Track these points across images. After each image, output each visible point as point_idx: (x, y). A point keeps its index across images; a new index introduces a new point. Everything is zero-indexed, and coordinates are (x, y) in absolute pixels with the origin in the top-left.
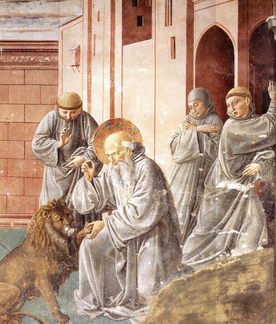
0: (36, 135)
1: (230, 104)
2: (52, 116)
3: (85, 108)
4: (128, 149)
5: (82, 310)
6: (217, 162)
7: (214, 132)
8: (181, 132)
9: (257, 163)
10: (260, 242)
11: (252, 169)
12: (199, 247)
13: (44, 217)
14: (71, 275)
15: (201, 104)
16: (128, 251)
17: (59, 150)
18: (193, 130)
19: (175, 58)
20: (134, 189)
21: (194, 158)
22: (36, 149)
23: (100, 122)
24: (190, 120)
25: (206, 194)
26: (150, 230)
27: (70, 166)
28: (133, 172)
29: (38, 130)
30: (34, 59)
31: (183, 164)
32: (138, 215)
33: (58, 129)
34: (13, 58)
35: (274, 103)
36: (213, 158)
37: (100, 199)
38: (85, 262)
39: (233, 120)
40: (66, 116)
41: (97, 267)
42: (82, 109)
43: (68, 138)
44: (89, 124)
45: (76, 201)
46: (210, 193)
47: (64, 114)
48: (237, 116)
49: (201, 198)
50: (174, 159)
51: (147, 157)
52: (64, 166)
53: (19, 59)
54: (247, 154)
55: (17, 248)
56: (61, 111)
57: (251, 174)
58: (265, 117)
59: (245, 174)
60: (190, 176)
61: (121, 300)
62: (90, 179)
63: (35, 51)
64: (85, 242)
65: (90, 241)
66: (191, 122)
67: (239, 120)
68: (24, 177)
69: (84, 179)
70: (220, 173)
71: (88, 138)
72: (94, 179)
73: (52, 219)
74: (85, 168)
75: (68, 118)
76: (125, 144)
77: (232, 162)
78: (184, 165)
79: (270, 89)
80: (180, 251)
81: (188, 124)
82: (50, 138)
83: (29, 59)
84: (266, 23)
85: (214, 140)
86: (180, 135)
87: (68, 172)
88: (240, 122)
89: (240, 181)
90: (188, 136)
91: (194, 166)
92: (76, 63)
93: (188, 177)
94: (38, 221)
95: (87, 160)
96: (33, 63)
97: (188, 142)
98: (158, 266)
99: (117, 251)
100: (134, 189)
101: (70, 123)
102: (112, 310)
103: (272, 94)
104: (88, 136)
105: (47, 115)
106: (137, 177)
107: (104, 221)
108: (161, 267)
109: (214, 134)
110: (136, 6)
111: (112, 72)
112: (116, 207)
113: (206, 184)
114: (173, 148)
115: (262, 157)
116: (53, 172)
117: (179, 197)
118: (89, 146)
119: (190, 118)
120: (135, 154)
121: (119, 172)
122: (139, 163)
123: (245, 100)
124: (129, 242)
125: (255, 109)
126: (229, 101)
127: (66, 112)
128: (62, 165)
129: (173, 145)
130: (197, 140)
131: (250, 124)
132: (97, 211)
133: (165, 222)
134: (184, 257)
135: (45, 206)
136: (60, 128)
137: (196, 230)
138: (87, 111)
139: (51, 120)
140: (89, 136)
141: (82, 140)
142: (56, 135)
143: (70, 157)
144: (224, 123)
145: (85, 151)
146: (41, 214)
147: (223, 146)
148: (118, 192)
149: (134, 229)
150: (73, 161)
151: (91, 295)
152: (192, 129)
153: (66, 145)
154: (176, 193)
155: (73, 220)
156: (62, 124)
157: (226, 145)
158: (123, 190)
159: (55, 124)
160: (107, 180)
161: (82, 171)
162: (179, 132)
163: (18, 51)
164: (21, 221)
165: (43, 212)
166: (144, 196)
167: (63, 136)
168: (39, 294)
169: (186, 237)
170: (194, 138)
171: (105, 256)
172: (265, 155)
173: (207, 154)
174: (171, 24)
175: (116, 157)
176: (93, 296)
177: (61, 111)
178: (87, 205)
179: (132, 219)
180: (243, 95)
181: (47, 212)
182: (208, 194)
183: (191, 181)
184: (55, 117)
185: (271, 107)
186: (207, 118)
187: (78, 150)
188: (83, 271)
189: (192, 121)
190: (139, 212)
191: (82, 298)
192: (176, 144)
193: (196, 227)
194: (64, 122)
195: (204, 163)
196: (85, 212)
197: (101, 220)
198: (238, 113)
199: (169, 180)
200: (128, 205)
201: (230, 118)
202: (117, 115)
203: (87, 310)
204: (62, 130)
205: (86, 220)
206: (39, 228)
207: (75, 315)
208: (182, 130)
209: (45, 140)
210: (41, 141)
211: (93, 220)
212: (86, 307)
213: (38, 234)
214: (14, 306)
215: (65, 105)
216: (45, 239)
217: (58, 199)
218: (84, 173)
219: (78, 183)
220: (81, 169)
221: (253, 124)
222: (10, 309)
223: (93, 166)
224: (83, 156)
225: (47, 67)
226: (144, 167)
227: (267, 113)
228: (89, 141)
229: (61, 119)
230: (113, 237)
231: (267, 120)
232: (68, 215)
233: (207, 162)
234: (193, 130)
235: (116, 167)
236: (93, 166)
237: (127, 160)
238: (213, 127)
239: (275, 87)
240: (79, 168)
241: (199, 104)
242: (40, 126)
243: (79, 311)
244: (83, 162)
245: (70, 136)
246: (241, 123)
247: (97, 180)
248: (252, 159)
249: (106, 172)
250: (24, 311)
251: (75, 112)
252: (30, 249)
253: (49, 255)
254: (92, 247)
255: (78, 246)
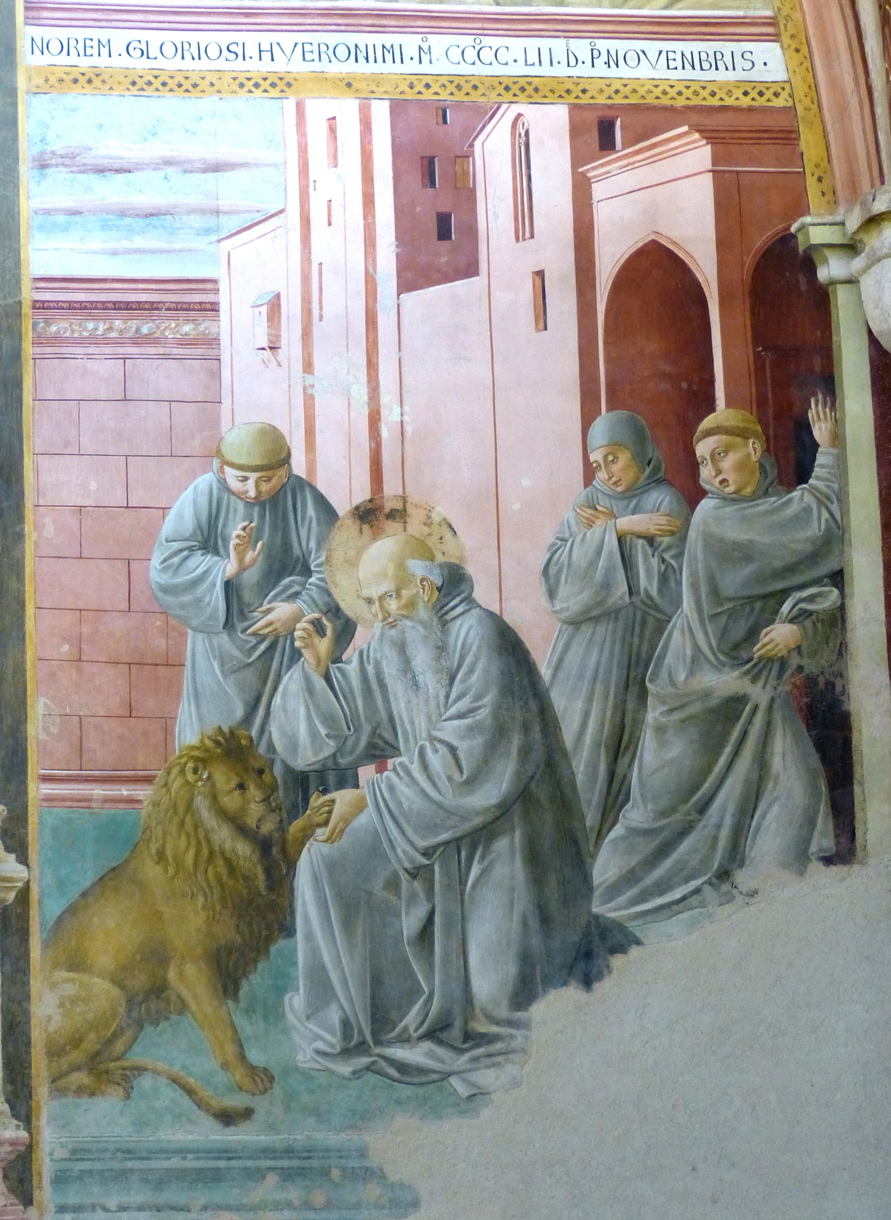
0: (160, 542)
1: (708, 457)
2: (207, 491)
3: (298, 465)
4: (425, 583)
5: (309, 1053)
6: (679, 622)
7: (665, 536)
8: (571, 535)
9: (791, 621)
10: (813, 848)
11: (778, 640)
12: (639, 864)
13: (190, 777)
14: (273, 949)
15: (624, 457)
16: (437, 876)
17: (228, 585)
18: (605, 530)
19: (546, 329)
20: (447, 696)
21: (613, 609)
22: (163, 582)
23: (342, 505)
24: (595, 502)
25: (654, 710)
26: (497, 814)
27: (261, 632)
28: (442, 649)
29: (168, 526)
30: (150, 329)
31: (584, 627)
32: (462, 772)
33: (224, 526)
34: (90, 325)
35: (831, 454)
36: (668, 609)
37: (352, 727)
38: (313, 912)
39: (718, 500)
40: (245, 488)
41: (348, 924)
42: (290, 469)
43: (254, 550)
44: (311, 512)
45: (283, 734)
46: (665, 708)
47: (240, 484)
48: (727, 490)
49: (638, 723)
50: (556, 612)
51: (480, 606)
52: (244, 631)
53: (109, 329)
54: (764, 597)
55: (114, 869)
56: (232, 476)
57: (776, 655)
58: (806, 494)
59: (759, 654)
60: (604, 660)
61: (423, 1023)
62: (322, 669)
63: (153, 307)
64: (312, 850)
65: (326, 848)
66: (599, 508)
67: (734, 500)
68: (130, 664)
69: (303, 666)
70: (689, 652)
71: (310, 553)
72: (333, 668)
73: (213, 785)
74: (304, 638)
75: (252, 493)
76: (417, 567)
77: (723, 619)
78: (587, 630)
79: (813, 417)
80: (586, 879)
81: (590, 511)
82: (200, 552)
83: (138, 330)
84: (793, 236)
85: (667, 556)
86: (569, 544)
87: (255, 647)
88: (738, 506)
89: (747, 673)
90: (592, 549)
91: (614, 631)
92: (270, 341)
93: (598, 663)
94: (173, 790)
95: (309, 614)
96: (150, 340)
97: (592, 564)
98: (525, 923)
99: (404, 877)
100: (447, 696)
101: (256, 509)
102: (399, 1053)
103: (820, 429)
104: (310, 546)
105: (191, 488)
106: (453, 663)
107: (365, 790)
108: (534, 924)
109: (666, 540)
110: (433, 184)
111: (372, 365)
112: (397, 749)
113: (651, 681)
114: (552, 581)
115: (803, 605)
116: (212, 647)
117: (577, 719)
118: (314, 574)
119: (594, 496)
120: (444, 597)
121: (402, 648)
122: (458, 622)
123: (747, 445)
124: (438, 853)
125: (776, 471)
126: (702, 449)
127: (245, 479)
128: (239, 629)
129: (552, 570)
130: (618, 556)
131: (765, 513)
132: (343, 761)
133: (542, 793)
134: (597, 893)
135: (193, 748)
136: (230, 523)
137: (628, 815)
138: (304, 477)
139: (204, 501)
140: (313, 545)
141: (295, 556)
142: (220, 542)
143: (261, 605)
144: (693, 509)
145: (304, 588)
146: (182, 772)
147: (694, 575)
148: (402, 705)
149: (450, 813)
150: (270, 617)
151: (334, 1007)
152: (604, 526)
153: (247, 571)
154: (566, 708)
155: (274, 788)
156: (236, 511)
157: (701, 573)
158: (415, 701)
159: (214, 513)
160: (370, 669)
161: (297, 644)
162: (567, 535)
163: (104, 306)
164: (124, 791)
165: (186, 763)
166: (477, 717)
167: (238, 545)
168: (183, 1008)
169: (600, 835)
170: (611, 554)
171: (370, 894)
172: (811, 599)
173: (650, 597)
174: (532, 236)
175: (393, 605)
176: (340, 1012)
177: (232, 476)
178: (313, 742)
179: (444, 784)
180: (743, 434)
181: (200, 766)
182: (659, 711)
183: (608, 671)
184: (215, 492)
185: (819, 464)
186: (646, 495)
187: (286, 581)
188: (309, 937)
189: (601, 503)
190: (464, 763)
191: (308, 1018)
192: (560, 571)
193: (628, 806)
194: (241, 506)
195: (644, 622)
196: (309, 765)
197: (357, 786)
198: (731, 482)
199: (545, 671)
200: (432, 744)
201: (710, 495)
202: (391, 487)
203: (325, 1054)
204: (236, 531)
205: (313, 786)
206: (176, 812)
207: (290, 1069)
208: (574, 528)
209: (187, 557)
210: (176, 560)
211: (332, 787)
212: (320, 1045)
213: (173, 829)
214: (109, 1042)
215: (243, 461)
216: (193, 843)
217: (230, 728)
218: (303, 651)
219: (285, 679)
220: (292, 642)
221: (774, 511)
222: (98, 1054)
223: (329, 632)
224: (299, 604)
225: (188, 351)
226: (472, 633)
227: (811, 481)
228: (314, 561)
229: (232, 497)
230: (392, 838)
231: (808, 499)
232: (261, 772)
233: (650, 620)
234: (605, 530)
235: (393, 632)
236: (329, 632)
237: (423, 612)
238: (663, 520)
239: (827, 410)
240: (289, 637)
241: (620, 456)
242: (171, 515)
243: (300, 1057)
244: (298, 618)
245: (260, 544)
246: (741, 509)
247: (339, 669)
248: (776, 612)
249: (366, 646)
250: (136, 1057)
251: (269, 479)
252: (151, 871)
253: (207, 890)
254: (332, 866)
255: (292, 865)
